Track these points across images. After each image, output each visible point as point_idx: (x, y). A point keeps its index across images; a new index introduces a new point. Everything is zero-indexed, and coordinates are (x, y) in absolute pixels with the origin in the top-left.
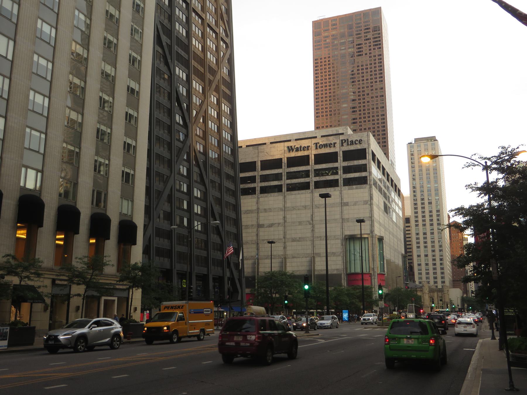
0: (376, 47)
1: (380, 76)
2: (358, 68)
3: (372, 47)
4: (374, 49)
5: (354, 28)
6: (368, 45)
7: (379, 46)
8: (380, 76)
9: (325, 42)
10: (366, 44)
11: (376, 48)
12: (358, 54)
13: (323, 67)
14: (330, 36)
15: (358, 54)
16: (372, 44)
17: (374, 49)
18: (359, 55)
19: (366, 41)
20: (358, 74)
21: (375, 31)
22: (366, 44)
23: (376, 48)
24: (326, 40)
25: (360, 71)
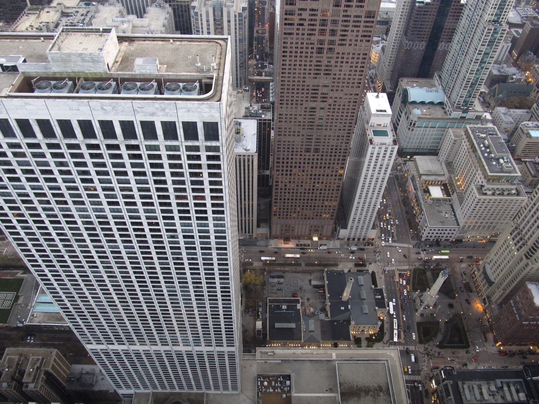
0: (364, 39)
1: (361, 73)
2: (337, 60)
3: (359, 38)
4: (361, 41)
5: (343, 6)
6: (355, 33)
7: (367, 38)
8: (361, 73)
9: (300, 17)
10: (353, 31)
11: (364, 41)
12: (340, 42)
13: (294, 50)
14: (308, 10)
15: (340, 42)
16: (360, 34)
17: (361, 41)
18: (341, 45)
19: (353, 29)
20: (336, 66)
21: (368, 17)
22: (353, 31)
23: (364, 41)
24: (301, 15)
25: (339, 64)
